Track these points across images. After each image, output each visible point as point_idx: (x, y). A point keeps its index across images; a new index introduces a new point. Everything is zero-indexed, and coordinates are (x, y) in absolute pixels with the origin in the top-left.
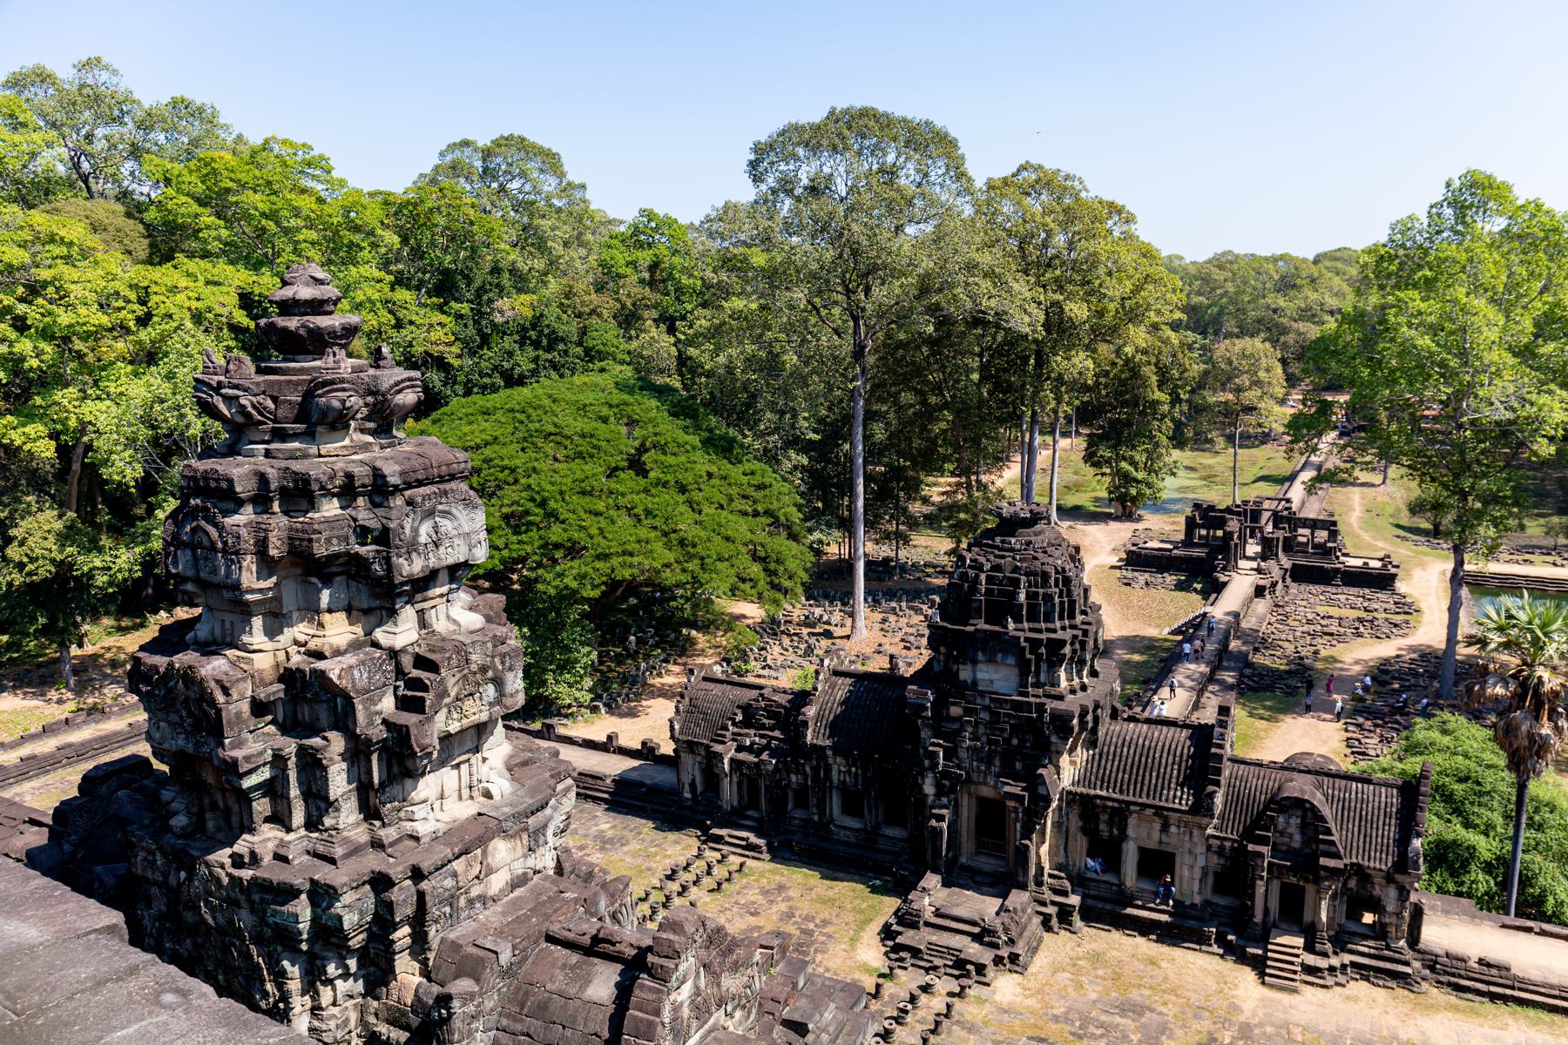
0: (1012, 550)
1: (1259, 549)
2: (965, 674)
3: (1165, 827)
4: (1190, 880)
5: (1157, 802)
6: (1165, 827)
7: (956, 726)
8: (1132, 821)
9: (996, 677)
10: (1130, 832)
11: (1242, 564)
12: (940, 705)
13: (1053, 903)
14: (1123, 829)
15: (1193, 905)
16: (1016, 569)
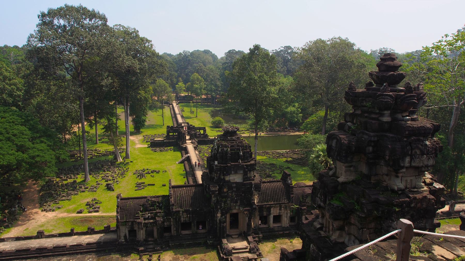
0: (234, 140)
1: (189, 137)
2: (227, 178)
3: (280, 209)
4: (285, 221)
5: (279, 202)
6: (280, 209)
7: (226, 194)
8: (272, 209)
9: (236, 178)
10: (272, 211)
11: (187, 141)
12: (220, 190)
13: (256, 237)
14: (270, 211)
15: (287, 227)
16: (238, 146)
